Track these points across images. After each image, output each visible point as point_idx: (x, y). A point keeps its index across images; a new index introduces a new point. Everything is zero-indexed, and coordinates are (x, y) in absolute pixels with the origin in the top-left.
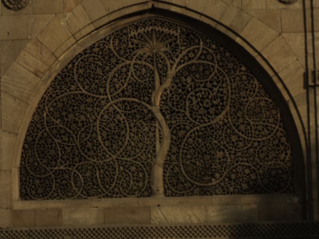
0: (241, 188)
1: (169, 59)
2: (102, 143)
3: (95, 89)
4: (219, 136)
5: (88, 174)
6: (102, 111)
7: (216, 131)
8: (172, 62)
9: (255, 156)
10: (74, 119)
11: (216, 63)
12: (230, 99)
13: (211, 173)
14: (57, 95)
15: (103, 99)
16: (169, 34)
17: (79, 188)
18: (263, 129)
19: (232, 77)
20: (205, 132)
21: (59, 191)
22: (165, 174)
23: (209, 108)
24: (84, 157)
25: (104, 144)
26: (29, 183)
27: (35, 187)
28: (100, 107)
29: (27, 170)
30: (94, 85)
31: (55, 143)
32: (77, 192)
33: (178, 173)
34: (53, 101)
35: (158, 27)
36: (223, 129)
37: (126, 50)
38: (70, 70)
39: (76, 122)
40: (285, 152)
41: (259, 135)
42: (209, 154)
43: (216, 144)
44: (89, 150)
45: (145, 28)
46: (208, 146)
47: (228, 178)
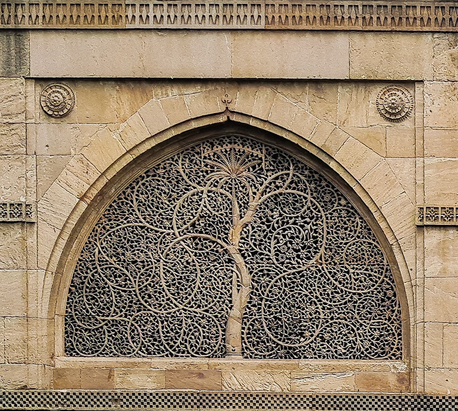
0: (336, 352)
1: (251, 186)
2: (166, 288)
3: (158, 222)
4: (311, 286)
5: (149, 326)
6: (168, 248)
7: (307, 279)
8: (255, 190)
9: (354, 312)
10: (133, 259)
11: (309, 194)
12: (325, 241)
13: (300, 331)
14: (111, 228)
15: (168, 234)
16: (252, 155)
17: (137, 344)
18: (365, 279)
19: (329, 212)
20: (295, 280)
21: (113, 347)
22: (243, 331)
23: (299, 250)
24: (144, 306)
25: (168, 290)
26: (76, 335)
27: (84, 340)
28: (164, 243)
29: (73, 319)
30: (157, 216)
31: (108, 287)
32: (135, 348)
33: (259, 330)
34: (106, 234)
35: (238, 145)
36: (316, 277)
37: (198, 173)
38: (128, 196)
39: (134, 262)
40: (391, 308)
41: (360, 286)
42: (297, 308)
43: (306, 296)
44: (150, 297)
45: (222, 147)
46: (297, 298)
47: (321, 337)
